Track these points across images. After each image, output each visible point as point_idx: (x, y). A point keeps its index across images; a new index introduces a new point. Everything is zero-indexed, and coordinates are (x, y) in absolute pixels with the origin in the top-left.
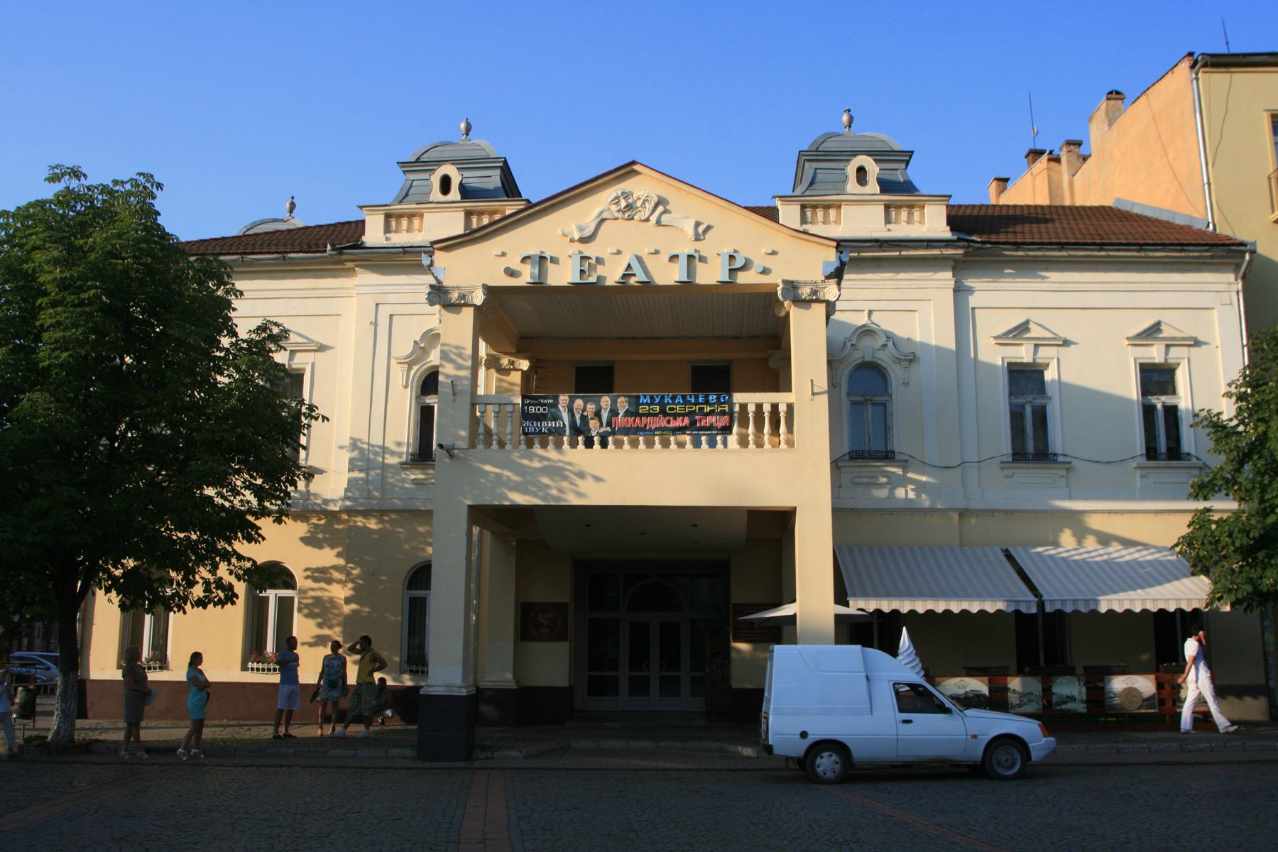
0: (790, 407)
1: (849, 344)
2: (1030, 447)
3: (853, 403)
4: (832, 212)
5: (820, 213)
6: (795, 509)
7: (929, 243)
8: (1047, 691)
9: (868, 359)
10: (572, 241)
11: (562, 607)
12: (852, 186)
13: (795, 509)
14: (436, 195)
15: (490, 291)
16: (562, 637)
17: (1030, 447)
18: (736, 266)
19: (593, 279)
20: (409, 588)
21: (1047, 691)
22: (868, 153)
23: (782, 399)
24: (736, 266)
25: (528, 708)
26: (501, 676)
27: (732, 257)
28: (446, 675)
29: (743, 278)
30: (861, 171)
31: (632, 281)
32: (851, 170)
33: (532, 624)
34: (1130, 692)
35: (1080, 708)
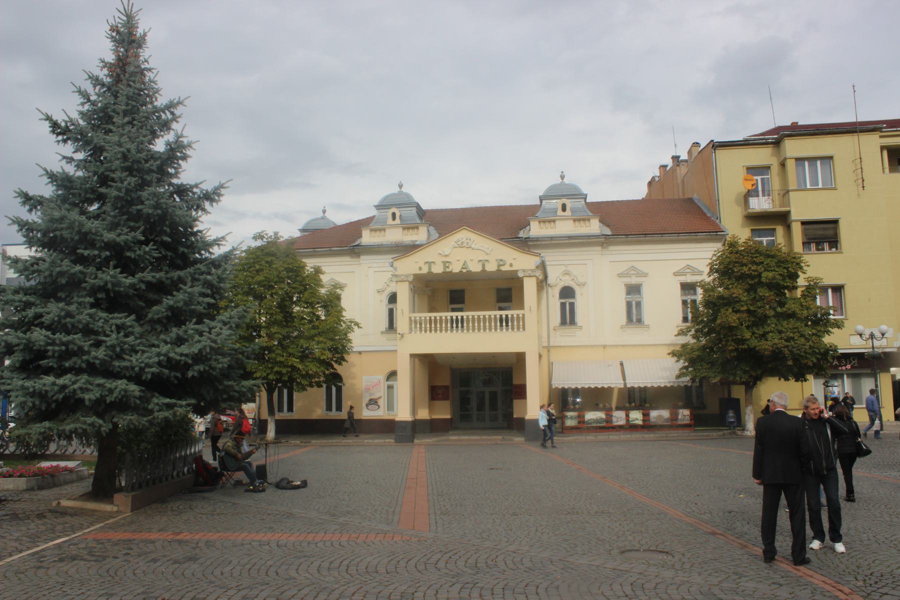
0: (523, 315)
2: (634, 319)
8: (627, 416)
11: (447, 387)
14: (390, 221)
15: (415, 275)
16: (446, 399)
17: (634, 319)
18: (501, 263)
20: (387, 380)
21: (627, 416)
23: (520, 312)
24: (501, 263)
25: (433, 427)
26: (424, 414)
28: (403, 413)
29: (503, 268)
31: (464, 271)
33: (435, 393)
34: (660, 417)
35: (640, 423)
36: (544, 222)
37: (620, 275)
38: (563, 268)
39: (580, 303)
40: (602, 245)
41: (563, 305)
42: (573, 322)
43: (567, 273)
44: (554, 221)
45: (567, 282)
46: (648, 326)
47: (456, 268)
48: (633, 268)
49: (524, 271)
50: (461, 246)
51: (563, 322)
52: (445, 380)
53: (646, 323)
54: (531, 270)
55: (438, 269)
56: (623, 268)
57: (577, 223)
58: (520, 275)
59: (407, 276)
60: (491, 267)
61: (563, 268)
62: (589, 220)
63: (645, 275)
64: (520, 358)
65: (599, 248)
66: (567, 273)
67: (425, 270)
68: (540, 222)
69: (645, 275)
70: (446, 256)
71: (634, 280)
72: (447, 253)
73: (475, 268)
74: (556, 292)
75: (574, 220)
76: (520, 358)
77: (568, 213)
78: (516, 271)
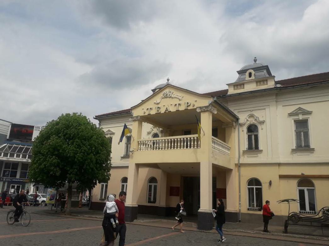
1: (246, 120)
3: (249, 135)
4: (242, 86)
5: (239, 87)
6: (200, 163)
7: (271, 89)
9: (252, 123)
10: (156, 104)
11: (178, 188)
12: (247, 78)
13: (200, 163)
19: (160, 112)
22: (252, 69)
27: (188, 103)
29: (189, 108)
30: (250, 75)
32: (247, 74)
36: (237, 85)
37: (290, 115)
38: (250, 113)
39: (262, 134)
40: (277, 95)
41: (250, 138)
42: (257, 147)
43: (252, 116)
44: (243, 84)
45: (252, 121)
46: (313, 149)
47: (163, 111)
48: (300, 109)
49: (200, 108)
50: (166, 97)
51: (250, 147)
52: (177, 183)
53: (311, 147)
54: (205, 107)
55: (153, 112)
56: (292, 109)
57: (259, 84)
58: (198, 110)
59: (137, 117)
60: (182, 108)
61: (250, 113)
62: (267, 80)
63: (310, 113)
64: (196, 166)
65: (274, 97)
66: (252, 116)
67: (146, 114)
68: (234, 86)
69: (310, 113)
70: (158, 104)
71: (301, 117)
72: (158, 102)
73: (173, 109)
74: (245, 129)
75: (257, 82)
76: (196, 166)
77: (253, 77)
78: (196, 109)
